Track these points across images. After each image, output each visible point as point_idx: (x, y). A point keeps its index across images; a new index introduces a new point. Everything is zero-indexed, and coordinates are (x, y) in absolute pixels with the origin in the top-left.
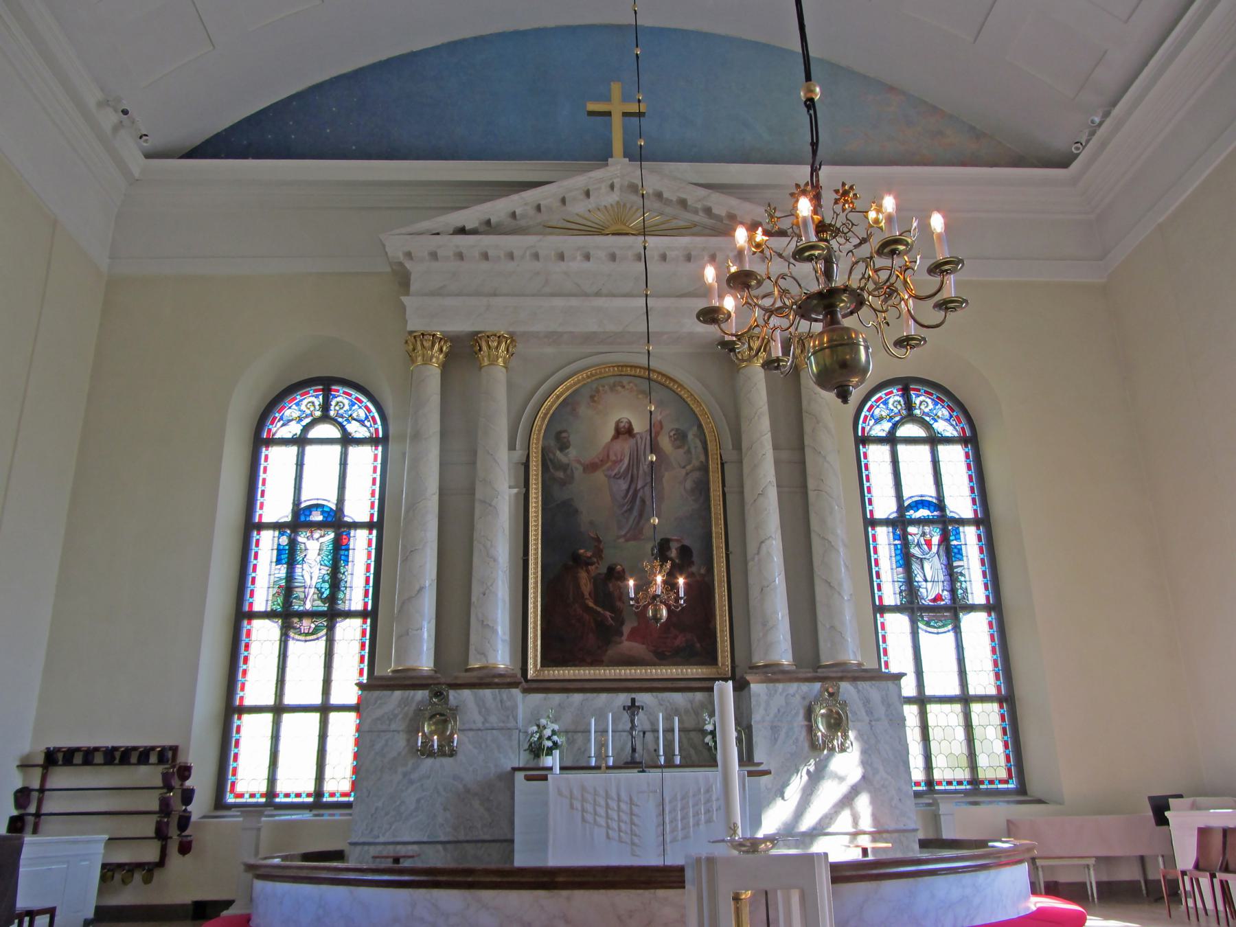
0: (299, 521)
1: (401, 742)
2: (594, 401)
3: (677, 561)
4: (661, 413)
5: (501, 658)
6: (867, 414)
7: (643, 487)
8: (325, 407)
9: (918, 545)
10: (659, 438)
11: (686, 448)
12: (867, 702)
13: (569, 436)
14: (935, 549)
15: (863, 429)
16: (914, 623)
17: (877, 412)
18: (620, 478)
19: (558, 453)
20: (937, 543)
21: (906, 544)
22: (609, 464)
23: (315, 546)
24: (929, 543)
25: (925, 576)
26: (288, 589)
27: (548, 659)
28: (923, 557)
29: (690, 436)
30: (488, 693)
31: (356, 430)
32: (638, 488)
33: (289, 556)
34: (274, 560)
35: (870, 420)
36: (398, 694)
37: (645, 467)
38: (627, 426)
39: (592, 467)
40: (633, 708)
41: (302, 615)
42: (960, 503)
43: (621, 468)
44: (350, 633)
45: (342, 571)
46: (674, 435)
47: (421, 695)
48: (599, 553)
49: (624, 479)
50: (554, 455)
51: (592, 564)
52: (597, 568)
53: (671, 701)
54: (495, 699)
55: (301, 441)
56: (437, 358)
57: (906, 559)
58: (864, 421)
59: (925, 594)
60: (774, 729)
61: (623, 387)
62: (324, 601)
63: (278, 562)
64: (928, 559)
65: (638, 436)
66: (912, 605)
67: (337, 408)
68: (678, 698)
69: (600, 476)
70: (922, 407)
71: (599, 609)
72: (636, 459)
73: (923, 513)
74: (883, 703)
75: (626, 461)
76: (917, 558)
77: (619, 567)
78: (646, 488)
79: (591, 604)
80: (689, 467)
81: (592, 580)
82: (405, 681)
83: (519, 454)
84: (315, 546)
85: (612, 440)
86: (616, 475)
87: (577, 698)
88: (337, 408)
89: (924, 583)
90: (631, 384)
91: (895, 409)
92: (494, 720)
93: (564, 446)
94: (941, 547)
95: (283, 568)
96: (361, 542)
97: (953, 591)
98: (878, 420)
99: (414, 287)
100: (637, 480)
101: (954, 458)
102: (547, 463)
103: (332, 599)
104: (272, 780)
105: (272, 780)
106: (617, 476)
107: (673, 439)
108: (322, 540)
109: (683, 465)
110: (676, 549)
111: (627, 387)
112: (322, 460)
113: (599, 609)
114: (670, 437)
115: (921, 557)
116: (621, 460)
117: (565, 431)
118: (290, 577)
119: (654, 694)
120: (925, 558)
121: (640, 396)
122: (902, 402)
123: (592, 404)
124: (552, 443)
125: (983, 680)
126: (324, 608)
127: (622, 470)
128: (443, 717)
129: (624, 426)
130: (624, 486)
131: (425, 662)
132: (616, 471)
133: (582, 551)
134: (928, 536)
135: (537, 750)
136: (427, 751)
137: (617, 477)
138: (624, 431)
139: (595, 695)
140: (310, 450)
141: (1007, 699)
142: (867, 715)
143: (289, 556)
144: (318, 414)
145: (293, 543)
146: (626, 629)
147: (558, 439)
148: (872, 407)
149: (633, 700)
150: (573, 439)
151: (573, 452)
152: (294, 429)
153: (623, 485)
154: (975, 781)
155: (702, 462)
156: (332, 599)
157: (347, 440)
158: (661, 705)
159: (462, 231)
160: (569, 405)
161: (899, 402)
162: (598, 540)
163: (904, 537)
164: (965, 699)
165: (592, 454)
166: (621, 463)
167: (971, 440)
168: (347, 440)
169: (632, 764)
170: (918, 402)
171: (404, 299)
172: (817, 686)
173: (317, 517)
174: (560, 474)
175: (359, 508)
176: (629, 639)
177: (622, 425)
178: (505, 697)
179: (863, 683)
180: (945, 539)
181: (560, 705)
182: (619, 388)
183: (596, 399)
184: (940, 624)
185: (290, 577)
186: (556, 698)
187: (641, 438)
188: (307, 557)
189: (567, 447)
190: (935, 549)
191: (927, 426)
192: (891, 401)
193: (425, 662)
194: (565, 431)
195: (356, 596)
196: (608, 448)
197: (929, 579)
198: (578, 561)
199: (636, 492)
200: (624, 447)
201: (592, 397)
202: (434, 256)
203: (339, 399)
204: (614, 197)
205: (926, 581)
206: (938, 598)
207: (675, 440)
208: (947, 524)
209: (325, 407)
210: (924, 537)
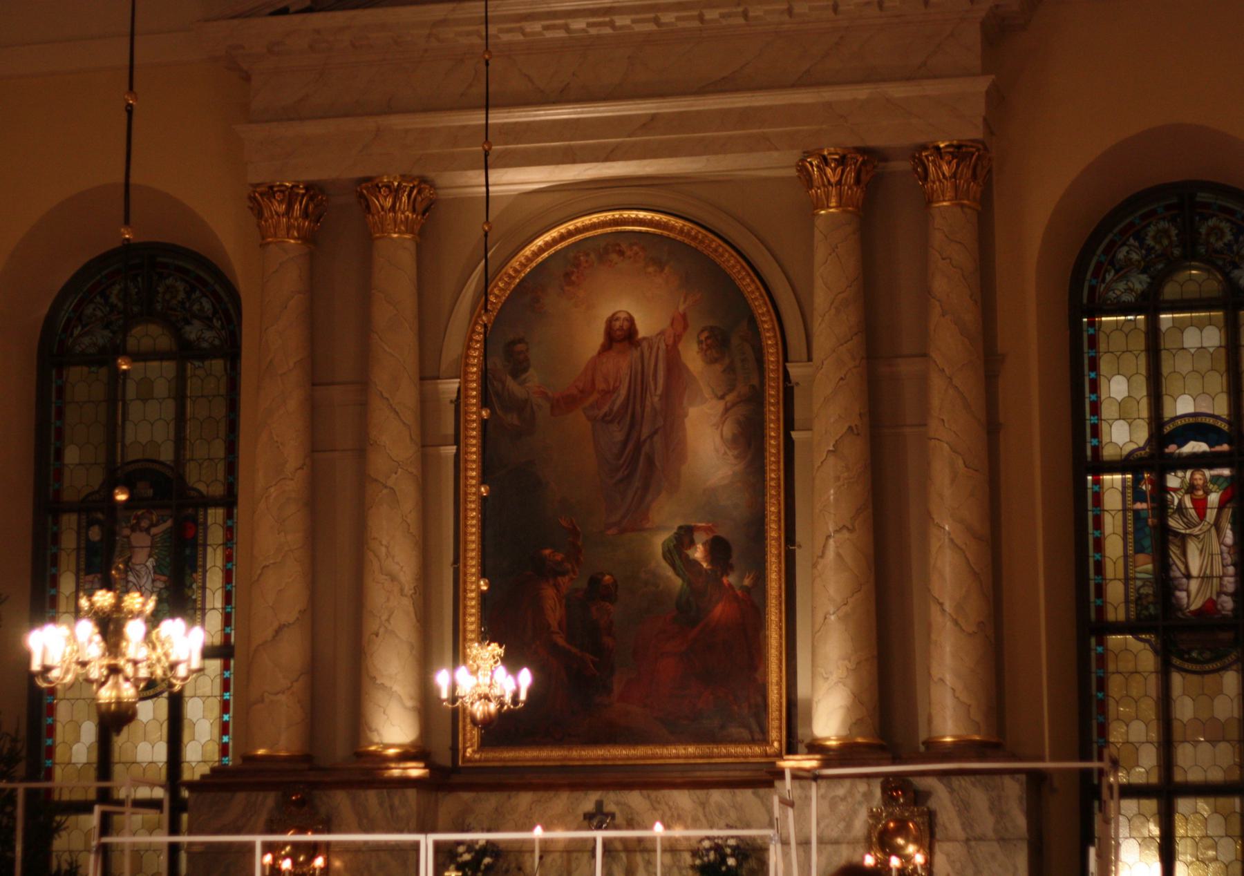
2: (572, 283)
3: (705, 565)
4: (685, 302)
6: (1103, 258)
7: (651, 436)
9: (1181, 509)
10: (680, 347)
11: (727, 361)
13: (527, 350)
14: (1211, 515)
15: (1092, 289)
17: (1122, 254)
18: (611, 421)
19: (511, 383)
20: (1216, 504)
22: (595, 396)
24: (1201, 506)
25: (1187, 567)
28: (1188, 531)
29: (735, 341)
32: (643, 438)
34: (83, 566)
35: (1107, 271)
37: (656, 399)
38: (626, 324)
39: (565, 403)
43: (613, 403)
45: (188, 584)
46: (707, 338)
49: (619, 423)
50: (503, 383)
51: (563, 574)
52: (572, 579)
53: (671, 804)
54: (381, 804)
58: (1095, 275)
59: (1185, 601)
61: (621, 253)
64: (1197, 536)
65: (645, 344)
67: (168, 297)
70: (1212, 240)
71: (574, 650)
74: (991, 810)
75: (623, 392)
76: (1176, 534)
77: (607, 577)
78: (656, 438)
80: (729, 398)
81: (564, 601)
85: (600, 353)
86: (605, 415)
88: (168, 297)
89: (1184, 580)
90: (635, 248)
91: (1157, 247)
93: (519, 367)
94: (1228, 513)
95: (96, 579)
98: (1123, 270)
100: (642, 425)
106: (609, 418)
107: (704, 347)
108: (154, 531)
109: (720, 394)
110: (704, 544)
111: (628, 253)
113: (574, 650)
114: (700, 342)
115: (1183, 531)
116: (616, 389)
117: (521, 341)
119: (645, 792)
120: (1190, 535)
121: (650, 269)
122: (1174, 232)
123: (567, 288)
124: (497, 362)
127: (615, 408)
129: (622, 327)
130: (619, 436)
132: (606, 409)
133: (547, 552)
134: (1201, 493)
139: (552, 794)
142: (964, 829)
148: (1112, 244)
149: (599, 804)
151: (534, 378)
153: (617, 434)
155: (753, 387)
158: (655, 809)
161: (1166, 232)
166: (616, 395)
170: (1203, 230)
174: (512, 419)
177: (617, 324)
178: (396, 802)
179: (960, 778)
181: (496, 809)
182: (614, 257)
183: (573, 278)
184: (1208, 655)
187: (651, 347)
188: (133, 560)
189: (525, 370)
190: (1211, 515)
192: (1152, 231)
194: (521, 341)
196: (594, 364)
197: (1194, 571)
199: (639, 446)
200: (621, 365)
201: (567, 275)
203: (169, 281)
205: (1188, 576)
207: (709, 347)
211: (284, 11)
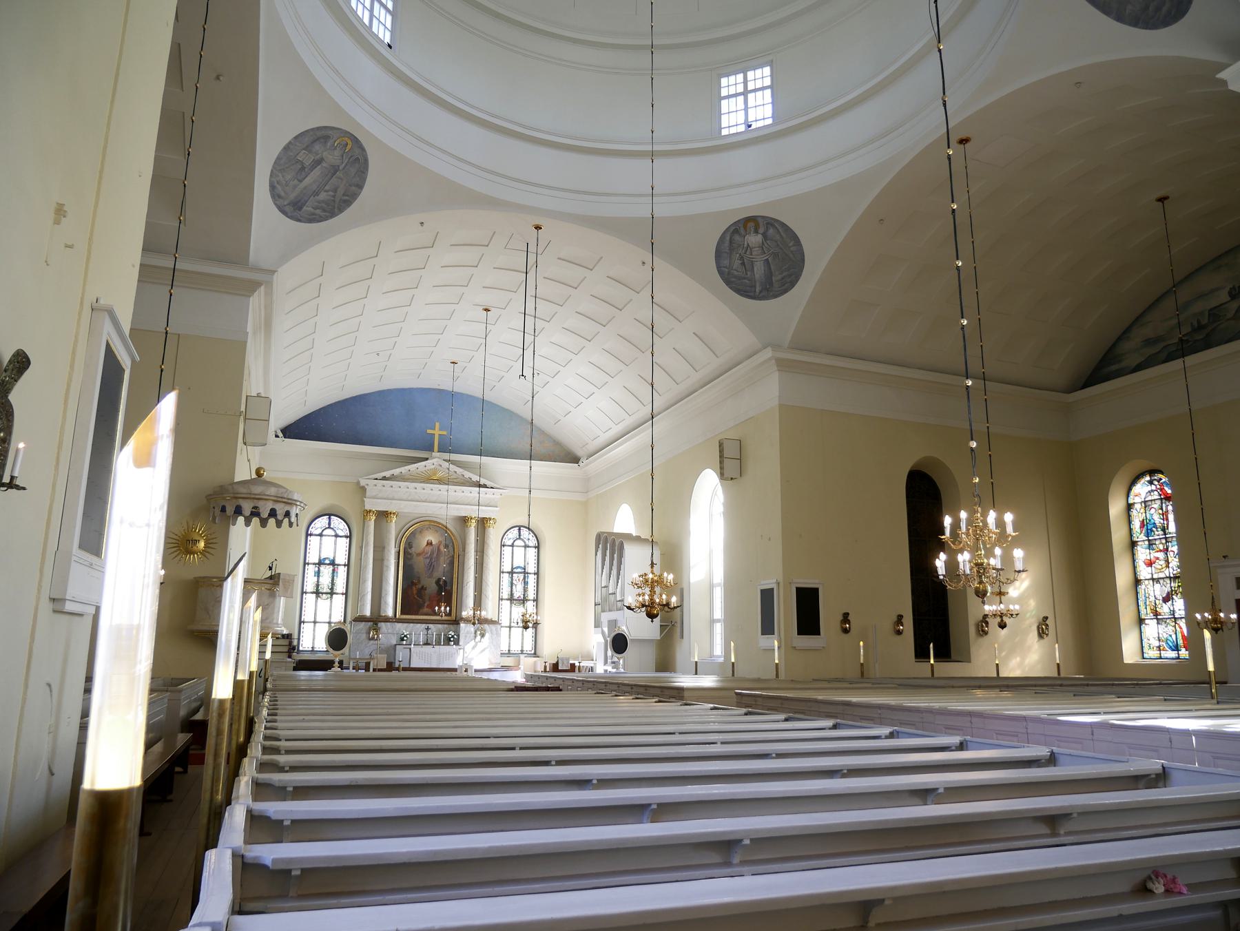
1: (364, 636)
5: (390, 613)
8: (329, 524)
16: (511, 603)
21: (512, 580)
27: (403, 613)
30: (389, 623)
33: (318, 574)
39: (419, 555)
40: (428, 629)
41: (322, 593)
42: (531, 568)
44: (339, 600)
48: (419, 581)
55: (321, 535)
56: (374, 518)
57: (512, 584)
62: (330, 589)
63: (315, 576)
68: (440, 626)
69: (421, 558)
72: (432, 553)
73: (519, 570)
79: (416, 596)
83: (397, 549)
84: (326, 571)
92: (390, 631)
93: (411, 547)
96: (342, 571)
101: (532, 553)
103: (332, 589)
112: (328, 542)
118: (318, 581)
124: (407, 546)
126: (330, 591)
128: (377, 630)
131: (368, 613)
136: (373, 639)
137: (426, 558)
138: (430, 544)
143: (318, 574)
144: (327, 526)
146: (426, 605)
147: (409, 545)
150: (413, 545)
152: (318, 532)
153: (428, 560)
156: (332, 589)
157: (337, 536)
159: (384, 478)
160: (413, 534)
162: (419, 578)
163: (512, 578)
165: (420, 550)
167: (538, 547)
168: (337, 536)
169: (427, 644)
171: (365, 499)
173: (327, 562)
174: (409, 556)
175: (341, 559)
176: (427, 607)
185: (318, 581)
193: (368, 613)
195: (311, 570)
196: (424, 549)
198: (413, 584)
200: (429, 549)
201: (420, 532)
204: (433, 467)
206: (520, 597)
208: (525, 573)
209: (329, 524)
210: (518, 578)
211: (376, 479)
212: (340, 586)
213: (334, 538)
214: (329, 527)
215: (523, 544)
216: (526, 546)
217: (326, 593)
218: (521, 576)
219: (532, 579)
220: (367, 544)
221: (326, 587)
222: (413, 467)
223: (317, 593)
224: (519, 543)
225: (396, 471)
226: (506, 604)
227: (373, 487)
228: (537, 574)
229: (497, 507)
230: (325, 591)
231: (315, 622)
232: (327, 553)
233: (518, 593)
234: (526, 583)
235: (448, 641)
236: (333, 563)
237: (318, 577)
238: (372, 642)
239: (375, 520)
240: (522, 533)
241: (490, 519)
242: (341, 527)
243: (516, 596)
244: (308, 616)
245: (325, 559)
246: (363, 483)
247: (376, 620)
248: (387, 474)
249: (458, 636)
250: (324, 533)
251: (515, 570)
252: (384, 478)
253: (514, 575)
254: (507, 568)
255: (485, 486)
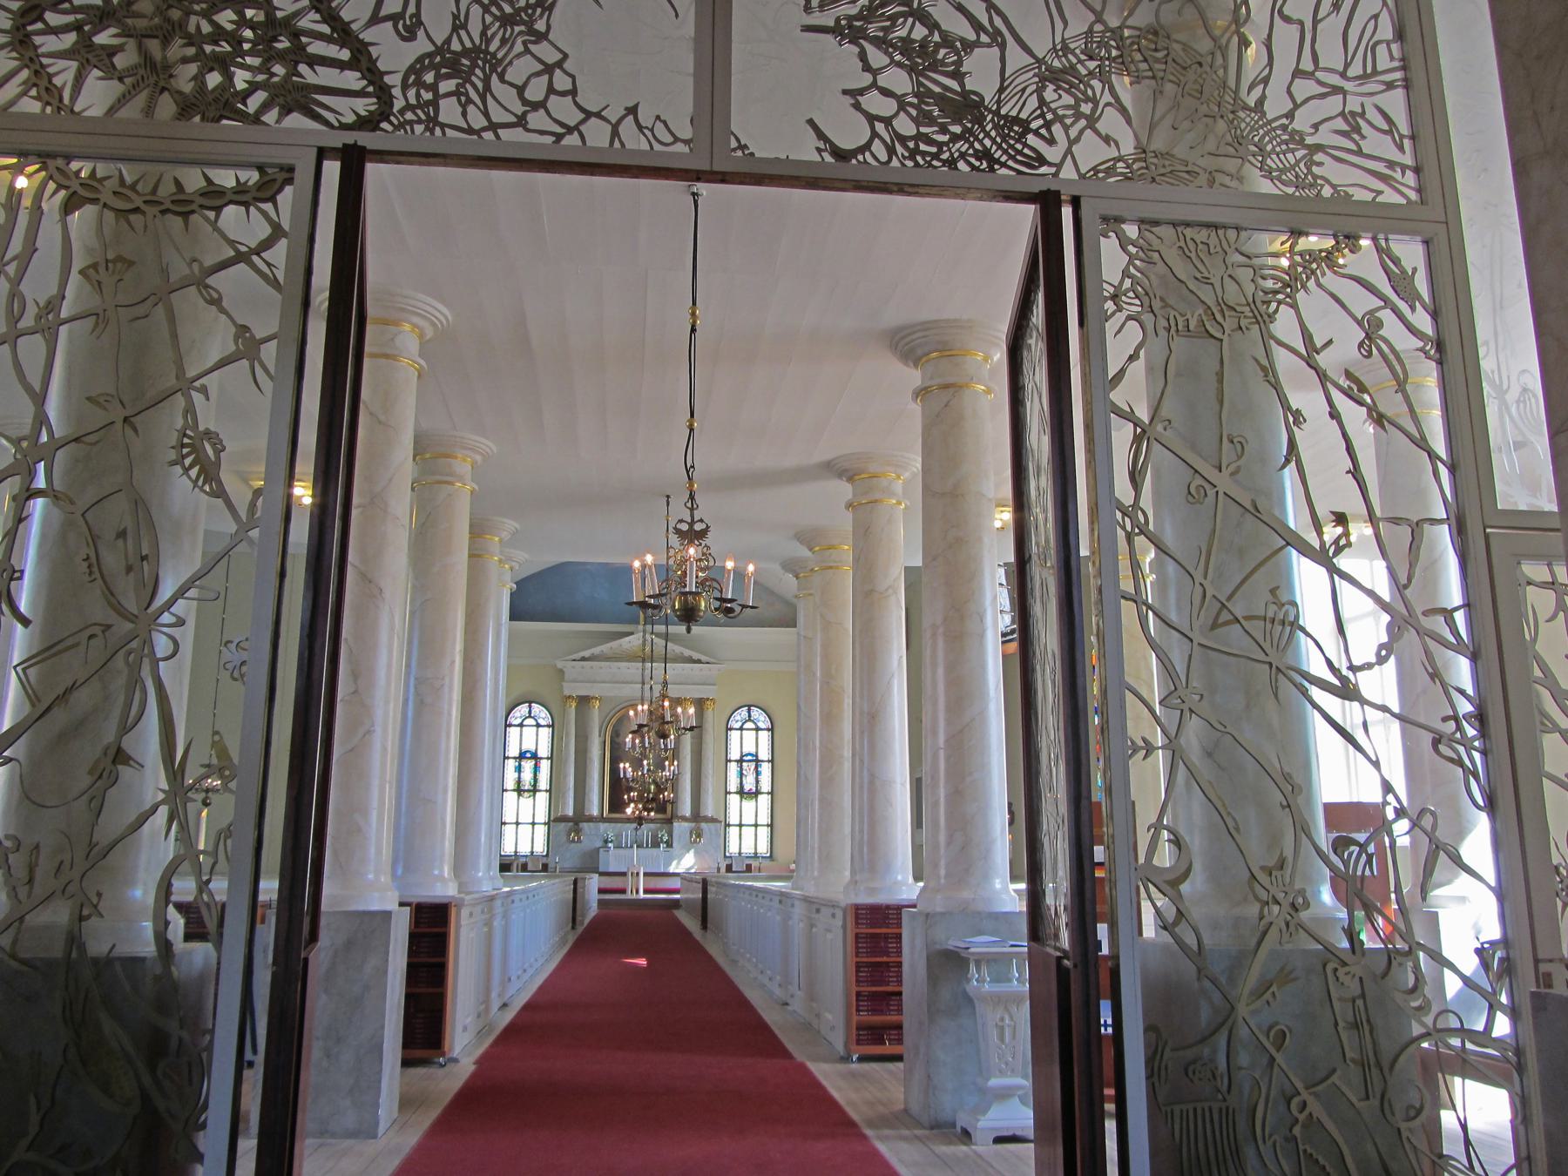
0: (522, 756)
5: (595, 812)
8: (530, 712)
12: (710, 829)
23: (528, 766)
26: (519, 781)
27: (611, 811)
30: (591, 824)
31: (542, 722)
33: (519, 769)
36: (563, 824)
41: (525, 791)
42: (764, 754)
44: (542, 798)
47: (571, 824)
55: (521, 725)
56: (574, 705)
57: (741, 775)
60: (680, 837)
66: (741, 792)
73: (749, 758)
82: (563, 819)
84: (528, 766)
87: (619, 825)
96: (545, 766)
97: (757, 787)
99: (567, 676)
101: (764, 736)
102: (612, 742)
103: (535, 785)
104: (532, 847)
105: (532, 847)
112: (529, 732)
118: (519, 778)
125: (764, 818)
128: (578, 831)
131: (570, 813)
135: (606, 842)
136: (573, 841)
140: (524, 728)
141: (771, 826)
143: (519, 769)
145: (520, 765)
152: (518, 721)
154: (756, 853)
157: (538, 725)
159: (583, 659)
163: (741, 767)
164: (756, 825)
167: (771, 730)
168: (538, 725)
172: (693, 824)
173: (528, 755)
175: (544, 751)
180: (756, 768)
185: (519, 778)
186: (613, 825)
191: (755, 724)
193: (570, 813)
202: (573, 667)
208: (757, 761)
209: (530, 712)
210: (749, 768)
212: (543, 783)
213: (535, 728)
214: (530, 716)
215: (534, 723)
216: (757, 729)
217: (528, 791)
218: (753, 765)
219: (766, 769)
220: (568, 735)
221: (527, 783)
222: (615, 644)
223: (519, 791)
224: (749, 725)
225: (596, 650)
226: (734, 800)
227: (572, 669)
228: (772, 761)
229: (714, 685)
230: (526, 788)
231: (517, 823)
232: (529, 745)
233: (749, 784)
234: (758, 773)
235: (656, 844)
236: (535, 756)
237: (520, 772)
238: (573, 845)
239: (576, 707)
240: (752, 714)
241: (708, 699)
242: (543, 715)
243: (747, 788)
244: (509, 816)
245: (526, 752)
246: (560, 665)
247: (579, 819)
248: (587, 654)
249: (671, 835)
250: (525, 723)
251: (745, 758)
252: (583, 659)
253: (744, 764)
254: (735, 754)
255: (699, 661)
